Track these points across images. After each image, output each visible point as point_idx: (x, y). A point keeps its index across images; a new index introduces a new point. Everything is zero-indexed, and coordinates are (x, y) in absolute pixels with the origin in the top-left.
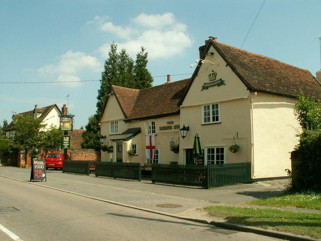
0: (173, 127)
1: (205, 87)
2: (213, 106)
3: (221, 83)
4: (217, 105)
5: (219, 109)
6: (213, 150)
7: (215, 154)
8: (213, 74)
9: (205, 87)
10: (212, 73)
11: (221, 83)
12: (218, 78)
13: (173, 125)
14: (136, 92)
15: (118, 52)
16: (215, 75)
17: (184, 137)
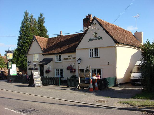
0: (71, 58)
1: (91, 40)
2: (95, 49)
3: (100, 38)
4: (97, 49)
5: (98, 51)
6: (58, 70)
7: (59, 72)
8: (95, 34)
9: (91, 40)
10: (95, 33)
11: (100, 38)
12: (98, 36)
13: (71, 58)
14: (46, 39)
15: (29, 16)
16: (96, 34)
17: (79, 64)
